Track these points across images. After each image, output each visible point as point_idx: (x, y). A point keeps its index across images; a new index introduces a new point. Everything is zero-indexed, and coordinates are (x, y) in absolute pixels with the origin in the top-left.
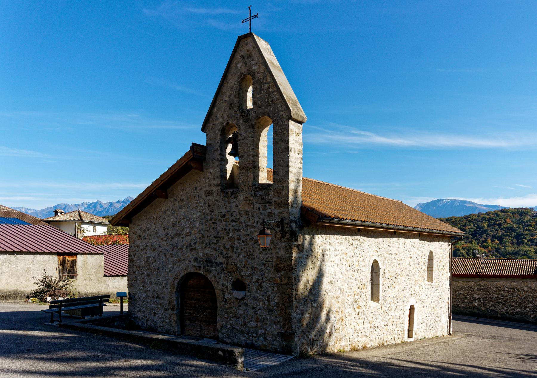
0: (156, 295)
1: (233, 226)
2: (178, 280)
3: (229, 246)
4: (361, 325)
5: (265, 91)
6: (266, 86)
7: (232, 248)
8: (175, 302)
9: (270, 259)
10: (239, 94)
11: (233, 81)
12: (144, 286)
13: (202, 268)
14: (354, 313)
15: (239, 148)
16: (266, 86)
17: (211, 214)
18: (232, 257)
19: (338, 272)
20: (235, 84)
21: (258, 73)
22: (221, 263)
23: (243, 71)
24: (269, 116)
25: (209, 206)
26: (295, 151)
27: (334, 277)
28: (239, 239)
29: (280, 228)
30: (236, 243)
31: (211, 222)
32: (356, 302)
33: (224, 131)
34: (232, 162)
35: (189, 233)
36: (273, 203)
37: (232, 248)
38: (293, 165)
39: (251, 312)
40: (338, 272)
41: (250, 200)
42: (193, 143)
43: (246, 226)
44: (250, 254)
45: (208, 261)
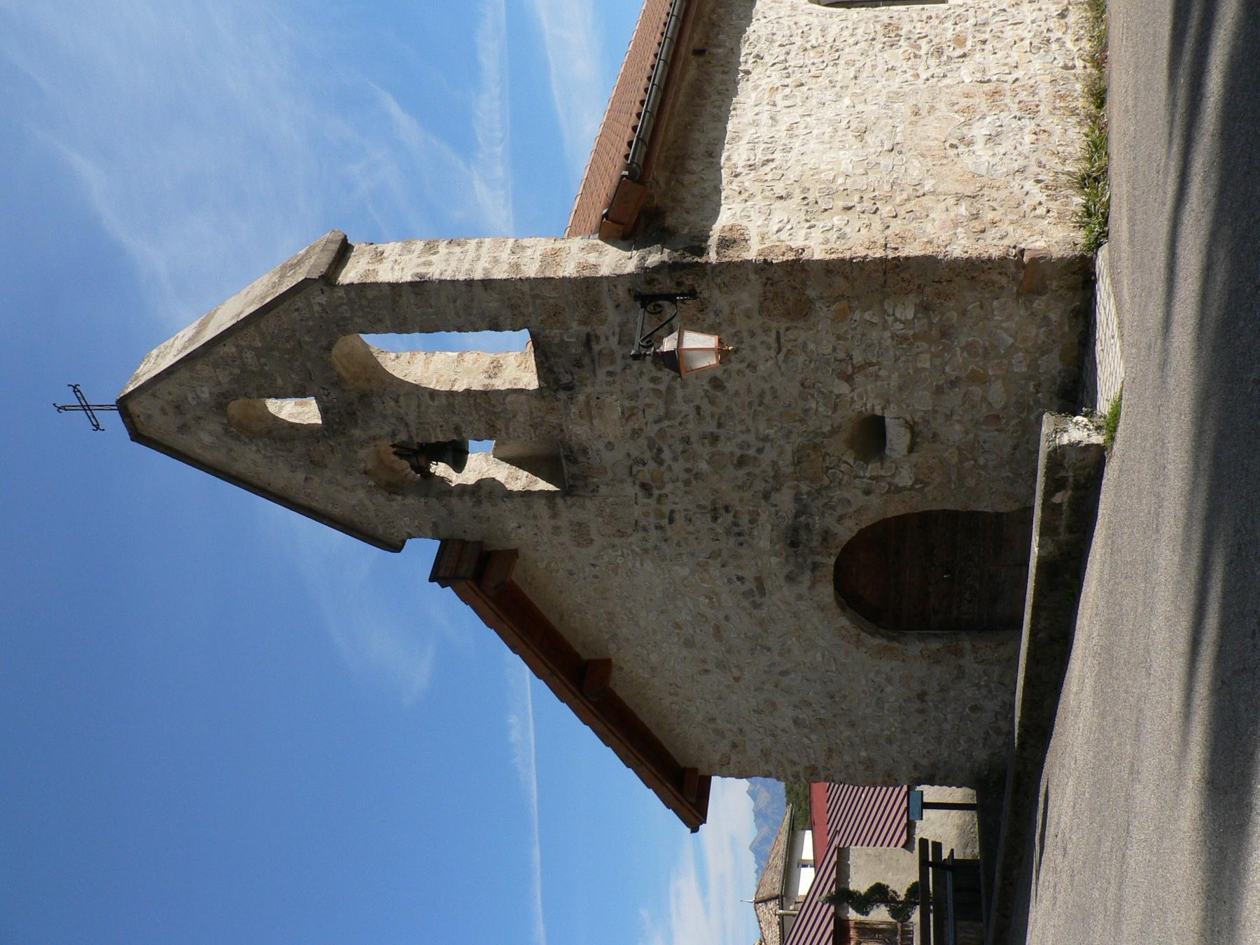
0: (917, 705)
1: (675, 459)
2: (863, 634)
3: (741, 473)
4: (1021, 31)
5: (263, 360)
6: (249, 356)
7: (742, 462)
8: (935, 645)
10: (282, 440)
11: (249, 458)
12: (890, 741)
13: (818, 558)
14: (978, 56)
15: (433, 441)
16: (249, 356)
17: (645, 529)
18: (774, 463)
19: (829, 113)
21: (219, 383)
22: (797, 498)
23: (219, 429)
24: (329, 349)
25: (621, 533)
26: (424, 264)
27: (844, 124)
28: (715, 439)
30: (727, 447)
31: (668, 527)
32: (939, 52)
33: (393, 488)
35: (711, 599)
36: (588, 329)
37: (742, 462)
38: (466, 266)
39: (953, 399)
40: (829, 113)
41: (587, 403)
42: (431, 580)
43: (668, 415)
45: (793, 539)
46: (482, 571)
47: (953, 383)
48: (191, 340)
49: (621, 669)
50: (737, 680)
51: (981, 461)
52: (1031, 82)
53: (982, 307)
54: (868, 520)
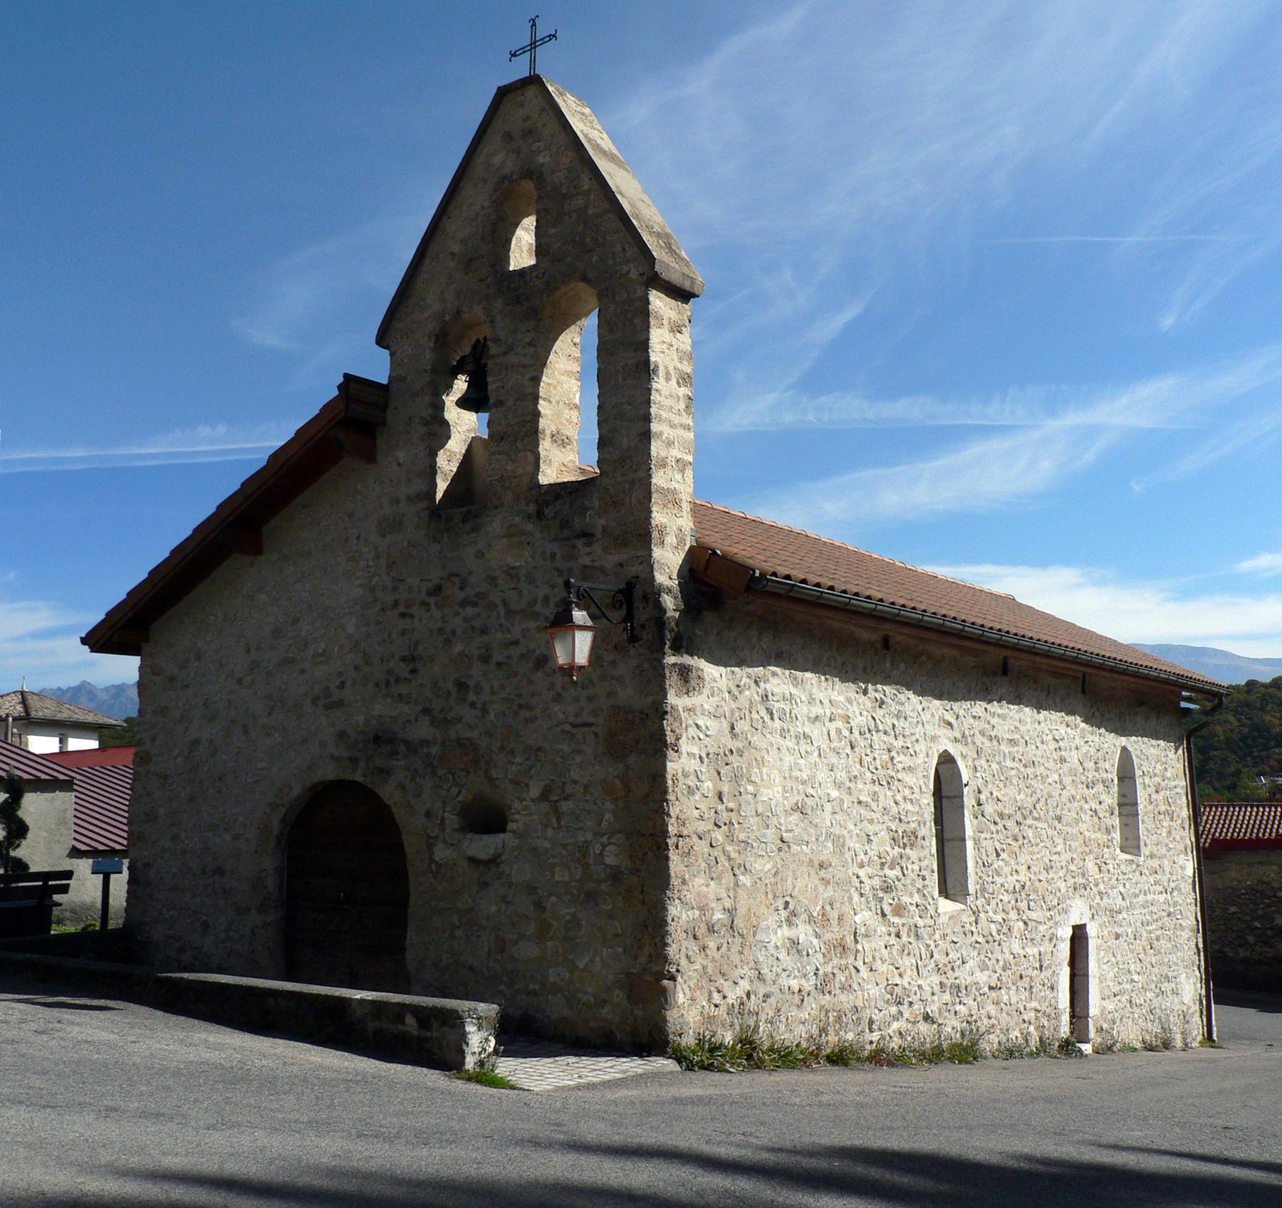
1: (466, 620)
3: (451, 686)
4: (910, 974)
5: (574, 216)
6: (579, 202)
7: (462, 686)
8: (271, 883)
9: (586, 718)
10: (494, 231)
11: (477, 199)
12: (175, 838)
13: (362, 764)
14: (883, 929)
15: (489, 379)
16: (579, 202)
17: (395, 589)
18: (459, 720)
19: (822, 775)
20: (483, 208)
21: (553, 172)
22: (424, 743)
23: (507, 171)
24: (585, 279)
25: (391, 565)
26: (668, 373)
27: (812, 792)
28: (485, 659)
29: (623, 612)
30: (477, 671)
31: (396, 612)
32: (887, 889)
33: (442, 339)
34: (465, 425)
35: (322, 655)
36: (598, 535)
37: (462, 686)
38: (664, 415)
40: (822, 775)
41: (523, 533)
42: (346, 376)
44: (520, 706)
45: (381, 739)
46: (355, 426)
47: (539, 905)
48: (597, 147)
49: (252, 565)
50: (240, 681)
51: (458, 933)
52: (856, 986)
53: (617, 935)
54: (399, 813)
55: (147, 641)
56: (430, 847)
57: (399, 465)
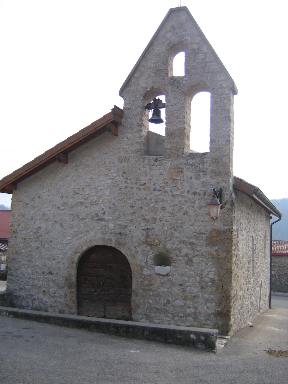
6: (202, 56)
49: (63, 167)
55: (16, 189)
56: (142, 270)
57: (128, 138)
